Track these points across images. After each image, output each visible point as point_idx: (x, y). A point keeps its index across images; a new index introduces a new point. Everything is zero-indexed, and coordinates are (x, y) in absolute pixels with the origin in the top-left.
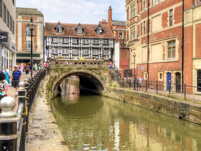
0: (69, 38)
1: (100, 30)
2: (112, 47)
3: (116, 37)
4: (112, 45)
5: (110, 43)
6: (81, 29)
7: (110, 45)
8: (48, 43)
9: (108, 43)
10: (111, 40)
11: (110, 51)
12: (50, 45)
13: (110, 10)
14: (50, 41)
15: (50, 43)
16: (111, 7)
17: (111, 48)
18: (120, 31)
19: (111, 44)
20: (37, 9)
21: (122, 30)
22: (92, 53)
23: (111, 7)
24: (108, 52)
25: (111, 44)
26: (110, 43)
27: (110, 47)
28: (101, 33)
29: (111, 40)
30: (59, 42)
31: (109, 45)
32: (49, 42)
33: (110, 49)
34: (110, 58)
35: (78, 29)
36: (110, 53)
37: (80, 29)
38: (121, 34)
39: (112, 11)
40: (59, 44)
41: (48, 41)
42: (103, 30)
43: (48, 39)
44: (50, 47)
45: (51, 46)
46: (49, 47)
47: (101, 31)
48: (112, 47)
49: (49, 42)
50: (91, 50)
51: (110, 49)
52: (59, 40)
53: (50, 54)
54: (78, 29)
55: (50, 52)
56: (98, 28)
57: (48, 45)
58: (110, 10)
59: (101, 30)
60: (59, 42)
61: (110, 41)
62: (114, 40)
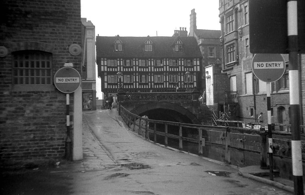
0: (134, 59)
2: (199, 70)
3: (204, 55)
4: (198, 67)
5: (195, 64)
6: (150, 44)
7: (195, 67)
9: (192, 64)
10: (197, 61)
11: (195, 77)
12: (106, 70)
13: (193, 14)
14: (106, 64)
15: (106, 67)
16: (194, 10)
17: (197, 72)
19: (197, 66)
20: (86, 19)
22: (167, 80)
23: (194, 10)
25: (197, 66)
26: (195, 64)
27: (195, 70)
29: (197, 61)
31: (193, 67)
33: (195, 74)
35: (147, 44)
36: (195, 80)
37: (148, 44)
38: (211, 50)
39: (197, 16)
43: (102, 62)
44: (105, 74)
45: (107, 72)
46: (104, 72)
49: (104, 66)
50: (167, 76)
51: (195, 74)
54: (147, 44)
58: (193, 14)
61: (195, 62)
62: (201, 59)
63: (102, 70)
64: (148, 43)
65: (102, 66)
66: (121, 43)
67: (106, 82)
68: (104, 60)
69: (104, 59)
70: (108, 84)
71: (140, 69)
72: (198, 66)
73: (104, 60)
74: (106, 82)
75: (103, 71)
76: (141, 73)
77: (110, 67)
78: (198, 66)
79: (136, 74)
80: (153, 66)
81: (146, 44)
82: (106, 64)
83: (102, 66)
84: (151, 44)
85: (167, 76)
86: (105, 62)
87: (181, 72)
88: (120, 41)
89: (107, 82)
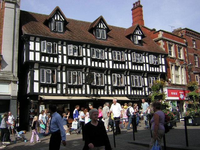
1: (137, 35)
2: (164, 71)
8: (31, 54)
12: (38, 59)
14: (38, 49)
15: (38, 55)
17: (162, 73)
22: (129, 84)
28: (139, 41)
30: (60, 53)
32: (35, 51)
35: (98, 28)
37: (101, 28)
41: (32, 48)
42: (143, 36)
43: (32, 44)
44: (36, 66)
46: (34, 62)
47: (140, 38)
48: (164, 71)
49: (35, 51)
52: (60, 49)
53: (36, 85)
55: (36, 78)
56: (135, 31)
57: (31, 58)
59: (139, 35)
63: (31, 58)
64: (100, 27)
65: (32, 51)
67: (36, 81)
72: (164, 65)
74: (36, 81)
75: (33, 60)
76: (69, 68)
78: (164, 65)
80: (111, 60)
81: (97, 27)
82: (38, 49)
83: (32, 51)
84: (104, 29)
85: (128, 77)
86: (38, 45)
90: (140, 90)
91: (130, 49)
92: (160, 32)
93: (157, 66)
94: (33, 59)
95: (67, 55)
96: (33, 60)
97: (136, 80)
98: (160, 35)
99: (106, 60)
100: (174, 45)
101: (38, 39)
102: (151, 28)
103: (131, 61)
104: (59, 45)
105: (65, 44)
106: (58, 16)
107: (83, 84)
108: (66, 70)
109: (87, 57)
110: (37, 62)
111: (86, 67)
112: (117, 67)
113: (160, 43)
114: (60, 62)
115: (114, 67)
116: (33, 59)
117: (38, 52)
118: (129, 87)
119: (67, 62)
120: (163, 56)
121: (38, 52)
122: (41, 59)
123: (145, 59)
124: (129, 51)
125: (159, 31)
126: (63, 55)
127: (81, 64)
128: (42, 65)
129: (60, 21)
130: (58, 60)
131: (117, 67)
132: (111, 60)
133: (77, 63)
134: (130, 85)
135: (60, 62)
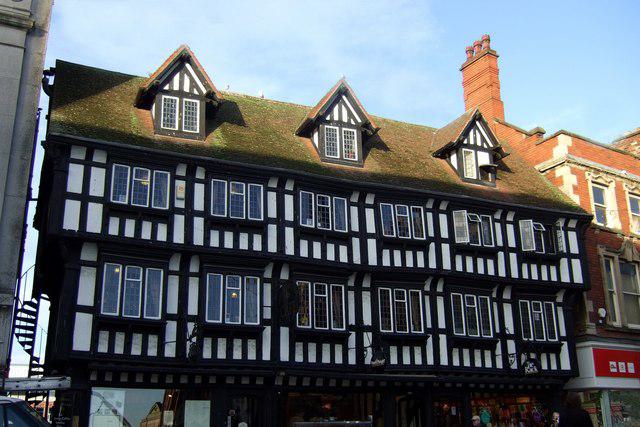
1: (476, 148)
2: (578, 279)
8: (72, 209)
12: (94, 225)
14: (97, 188)
15: (95, 211)
17: (571, 289)
18: (597, 171)
21: (606, 168)
22: (442, 324)
24: (550, 316)
30: (180, 204)
32: (85, 198)
34: (566, 365)
36: (563, 333)
37: (340, 123)
40: (179, 221)
41: (74, 184)
42: (497, 153)
43: (75, 173)
44: (89, 254)
45: (102, 241)
46: (82, 237)
47: (484, 159)
49: (85, 198)
50: (440, 302)
52: (181, 192)
56: (466, 134)
59: (482, 149)
60: (180, 204)
63: (71, 222)
65: (74, 196)
66: (196, 92)
67: (85, 309)
68: (88, 164)
69: (89, 155)
70: (101, 324)
71: (304, 244)
72: (575, 256)
73: (88, 164)
74: (85, 309)
75: (76, 229)
77: (124, 212)
78: (575, 256)
79: (185, 264)
80: (372, 236)
82: (97, 188)
83: (74, 196)
85: (440, 302)
86: (98, 176)
87: (438, 274)
88: (192, 80)
89: (93, 310)
90: (477, 348)
91: (445, 198)
92: (561, 137)
93: (553, 260)
94: (75, 227)
95: (205, 214)
96: (76, 229)
97: (470, 313)
98: (561, 149)
99: (355, 234)
100: (612, 185)
101: (100, 157)
102: (529, 128)
103: (451, 240)
104: (180, 178)
105: (200, 174)
106: (186, 77)
107: (264, 322)
108: (201, 268)
109: (281, 222)
110: (92, 238)
111: (279, 260)
112: (398, 263)
113: (561, 177)
114: (179, 238)
115: (386, 262)
116: (75, 227)
117: (96, 200)
118: (443, 338)
119: (207, 238)
120: (572, 224)
121: (96, 200)
122: (105, 224)
123: (502, 233)
124: (443, 206)
125: (556, 136)
126: (189, 213)
127: (257, 246)
128: (112, 249)
129: (190, 95)
130: (170, 233)
131: (398, 263)
132: (372, 236)
133: (146, 234)
134: (448, 331)
135: (179, 238)
